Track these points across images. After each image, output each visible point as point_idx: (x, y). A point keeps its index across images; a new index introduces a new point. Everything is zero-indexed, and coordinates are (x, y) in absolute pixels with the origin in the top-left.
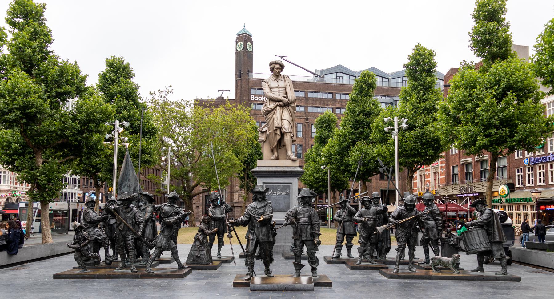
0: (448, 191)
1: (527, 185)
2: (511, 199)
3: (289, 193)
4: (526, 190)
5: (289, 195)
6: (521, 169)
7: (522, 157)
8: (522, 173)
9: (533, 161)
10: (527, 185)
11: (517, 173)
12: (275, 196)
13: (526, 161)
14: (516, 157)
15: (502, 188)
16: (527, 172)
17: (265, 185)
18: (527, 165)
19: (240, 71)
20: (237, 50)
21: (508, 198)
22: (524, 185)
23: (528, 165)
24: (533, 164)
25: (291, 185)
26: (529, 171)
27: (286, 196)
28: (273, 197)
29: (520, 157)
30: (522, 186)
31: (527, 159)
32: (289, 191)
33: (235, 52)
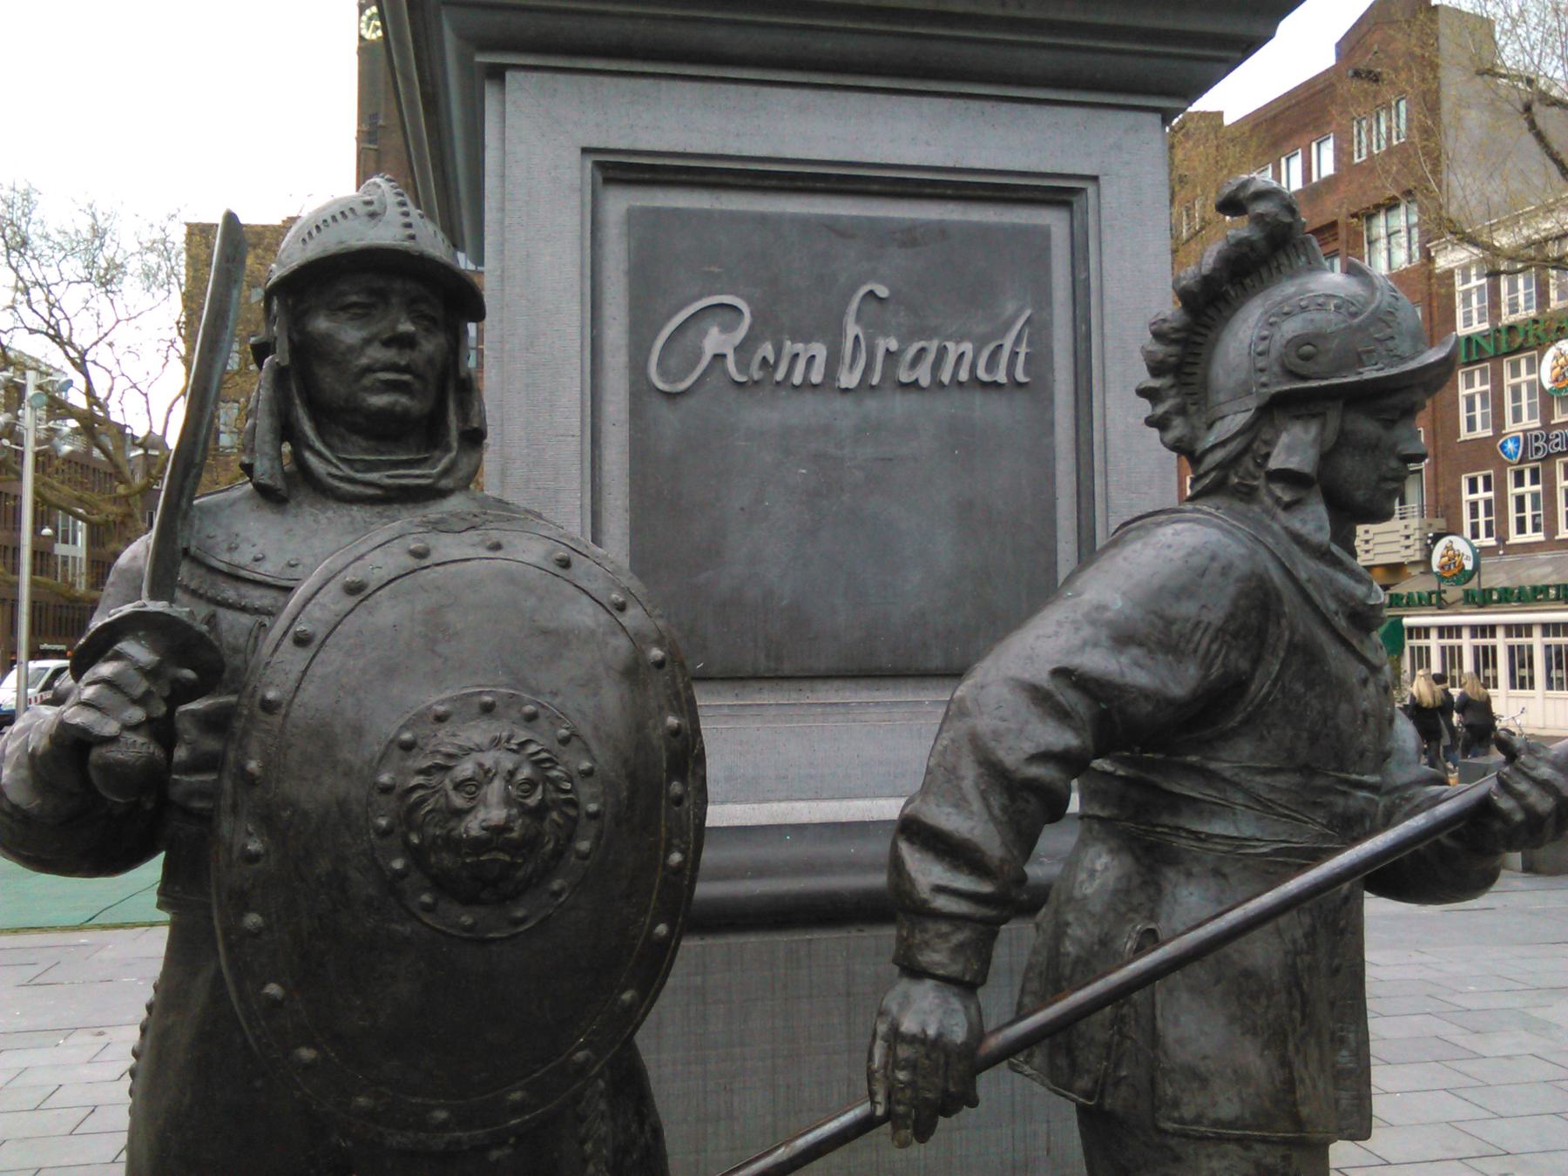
0: (1379, 549)
1: (1514, 538)
2: (1490, 591)
3: (1040, 360)
4: (1508, 559)
5: (1035, 388)
6: (1487, 479)
7: (1489, 433)
8: (1491, 494)
9: (1540, 443)
10: (1514, 538)
11: (1466, 496)
12: (808, 410)
13: (1510, 446)
14: (1464, 435)
15: (1448, 548)
16: (1512, 490)
17: (620, 202)
18: (1516, 460)
19: (374, 116)
20: (361, 38)
21: (1472, 585)
22: (1502, 539)
23: (1521, 462)
24: (1540, 455)
25: (1053, 221)
26: (1519, 482)
27: (983, 408)
28: (762, 415)
29: (1482, 432)
30: (1491, 542)
31: (1517, 440)
32: (1038, 330)
33: (354, 44)
